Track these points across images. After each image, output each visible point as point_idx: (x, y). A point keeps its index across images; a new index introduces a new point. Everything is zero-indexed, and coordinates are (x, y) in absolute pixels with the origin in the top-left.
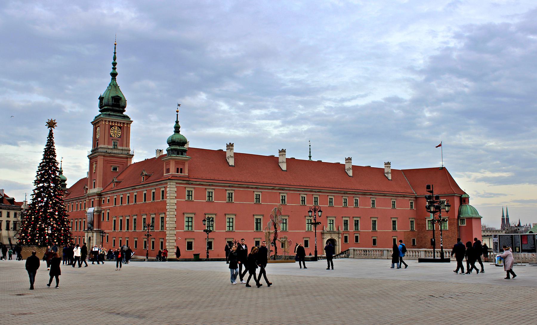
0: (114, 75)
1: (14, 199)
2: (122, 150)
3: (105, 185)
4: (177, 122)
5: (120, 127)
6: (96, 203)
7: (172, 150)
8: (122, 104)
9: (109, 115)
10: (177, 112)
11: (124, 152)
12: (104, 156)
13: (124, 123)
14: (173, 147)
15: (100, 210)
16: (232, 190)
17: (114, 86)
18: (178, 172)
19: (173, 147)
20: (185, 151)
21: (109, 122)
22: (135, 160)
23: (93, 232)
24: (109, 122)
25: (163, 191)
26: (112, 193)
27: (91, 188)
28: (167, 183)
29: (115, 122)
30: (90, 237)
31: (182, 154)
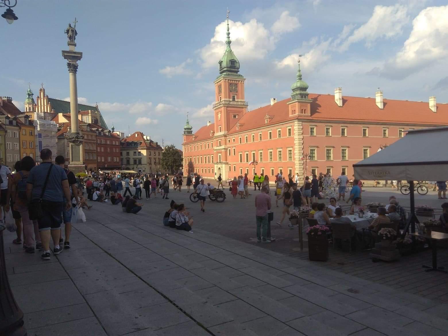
1: (157, 143)
3: (228, 128)
4: (300, 71)
5: (237, 84)
6: (223, 142)
7: (297, 94)
8: (237, 65)
9: (229, 75)
10: (299, 62)
13: (239, 81)
15: (226, 147)
16: (345, 126)
18: (302, 113)
19: (298, 92)
20: (307, 95)
21: (229, 80)
24: (229, 80)
25: (290, 129)
27: (217, 132)
29: (233, 80)
30: (219, 168)
31: (305, 98)
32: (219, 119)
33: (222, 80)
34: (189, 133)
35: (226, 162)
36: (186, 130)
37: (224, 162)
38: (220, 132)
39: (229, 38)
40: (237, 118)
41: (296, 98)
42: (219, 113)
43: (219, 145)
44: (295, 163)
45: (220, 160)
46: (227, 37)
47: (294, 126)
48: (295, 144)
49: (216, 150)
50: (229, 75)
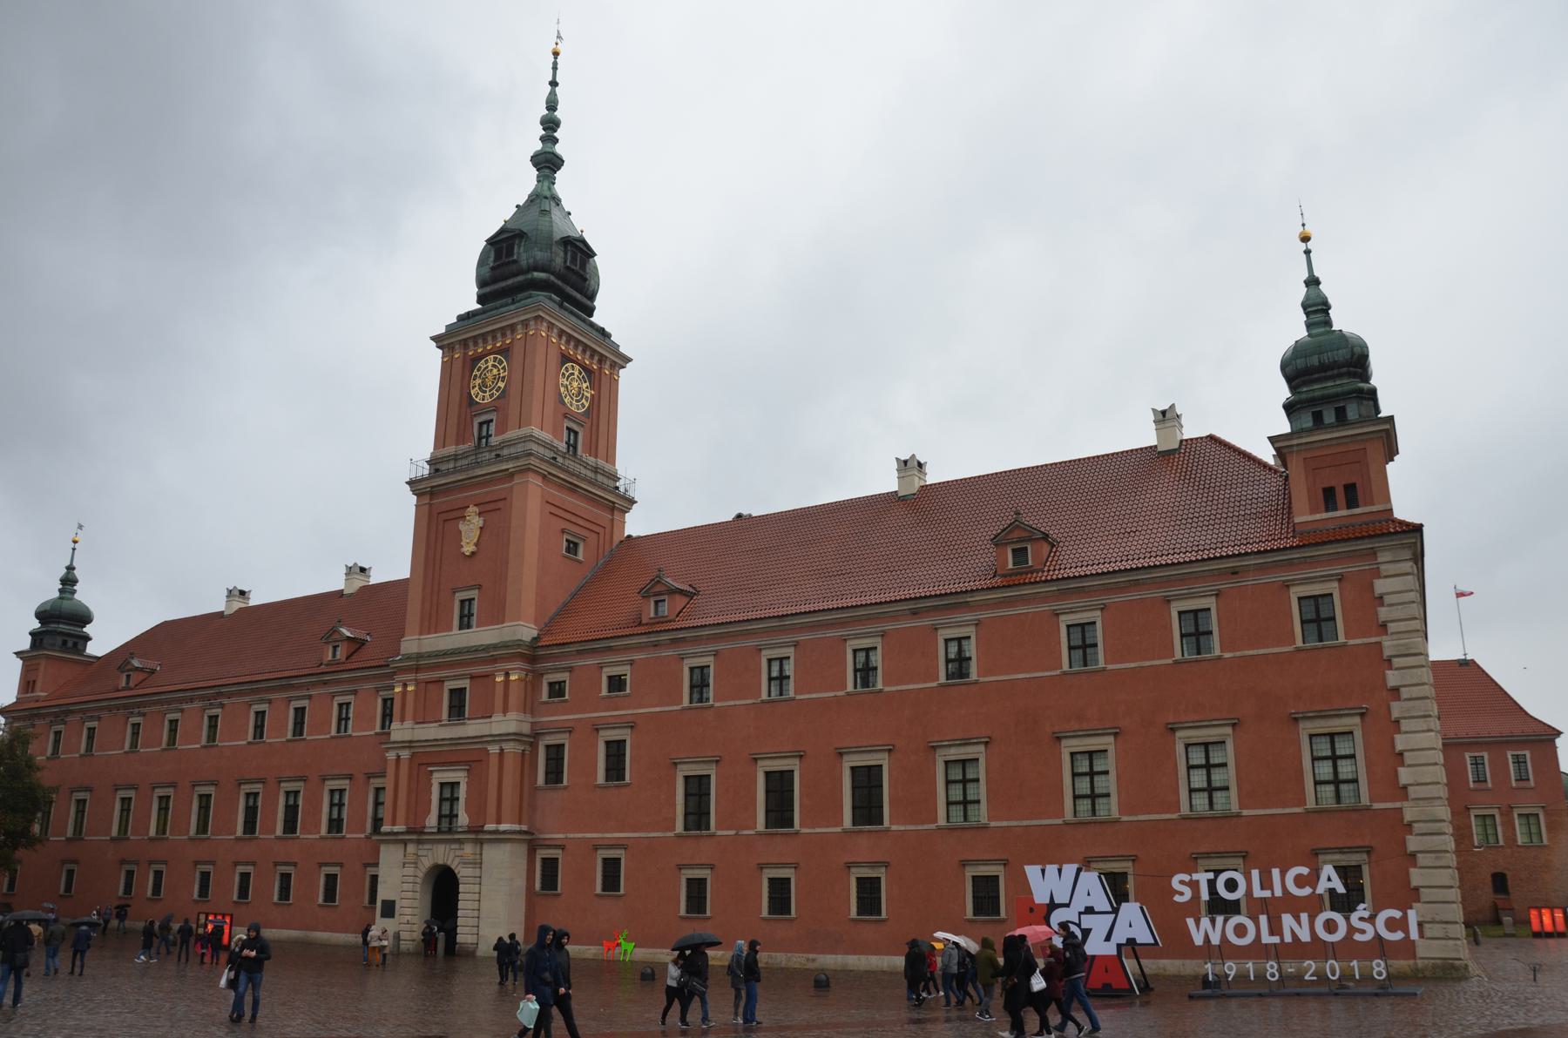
0: (547, 163)
2: (596, 470)
4: (1313, 282)
10: (1305, 239)
11: (600, 478)
12: (544, 477)
13: (602, 359)
14: (1317, 389)
15: (526, 729)
17: (543, 200)
21: (561, 333)
22: (636, 524)
23: (481, 842)
24: (561, 333)
26: (656, 645)
27: (433, 622)
28: (1373, 553)
32: (468, 549)
33: (525, 324)
34: (70, 644)
35: (516, 827)
36: (53, 626)
37: (503, 827)
38: (456, 631)
39: (556, 141)
40: (580, 557)
41: (1352, 412)
42: (472, 509)
43: (445, 715)
44: (1408, 817)
45: (449, 817)
46: (542, 139)
47: (1377, 574)
48: (1396, 691)
49: (409, 744)
50: (561, 306)
